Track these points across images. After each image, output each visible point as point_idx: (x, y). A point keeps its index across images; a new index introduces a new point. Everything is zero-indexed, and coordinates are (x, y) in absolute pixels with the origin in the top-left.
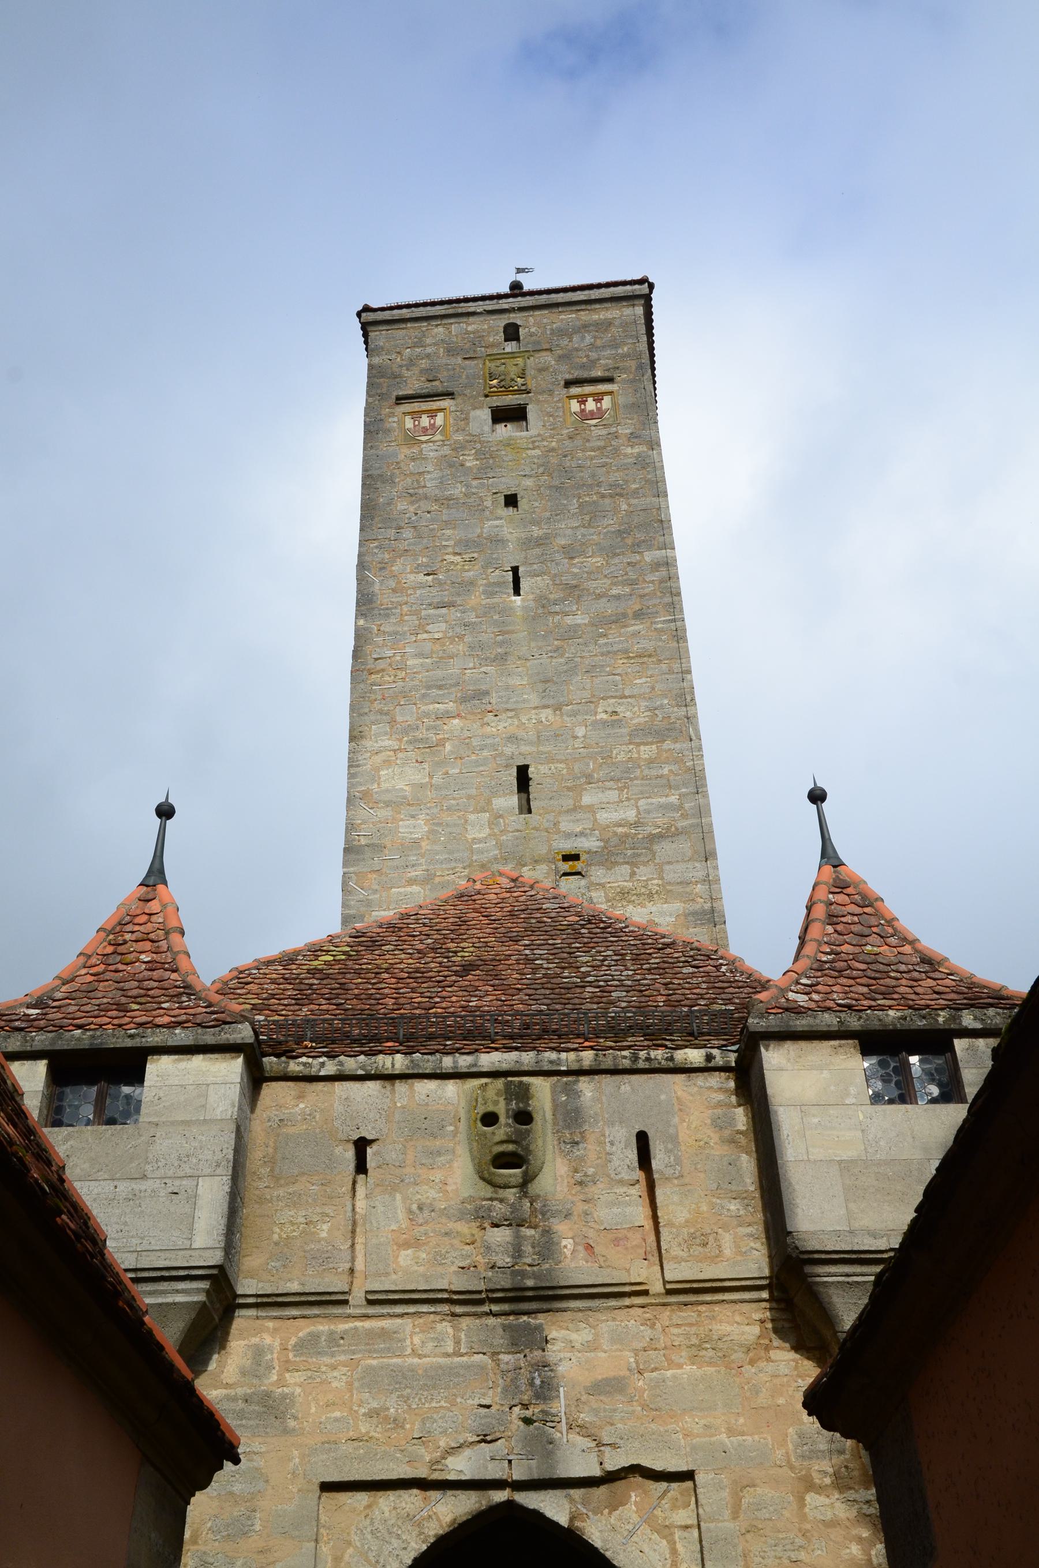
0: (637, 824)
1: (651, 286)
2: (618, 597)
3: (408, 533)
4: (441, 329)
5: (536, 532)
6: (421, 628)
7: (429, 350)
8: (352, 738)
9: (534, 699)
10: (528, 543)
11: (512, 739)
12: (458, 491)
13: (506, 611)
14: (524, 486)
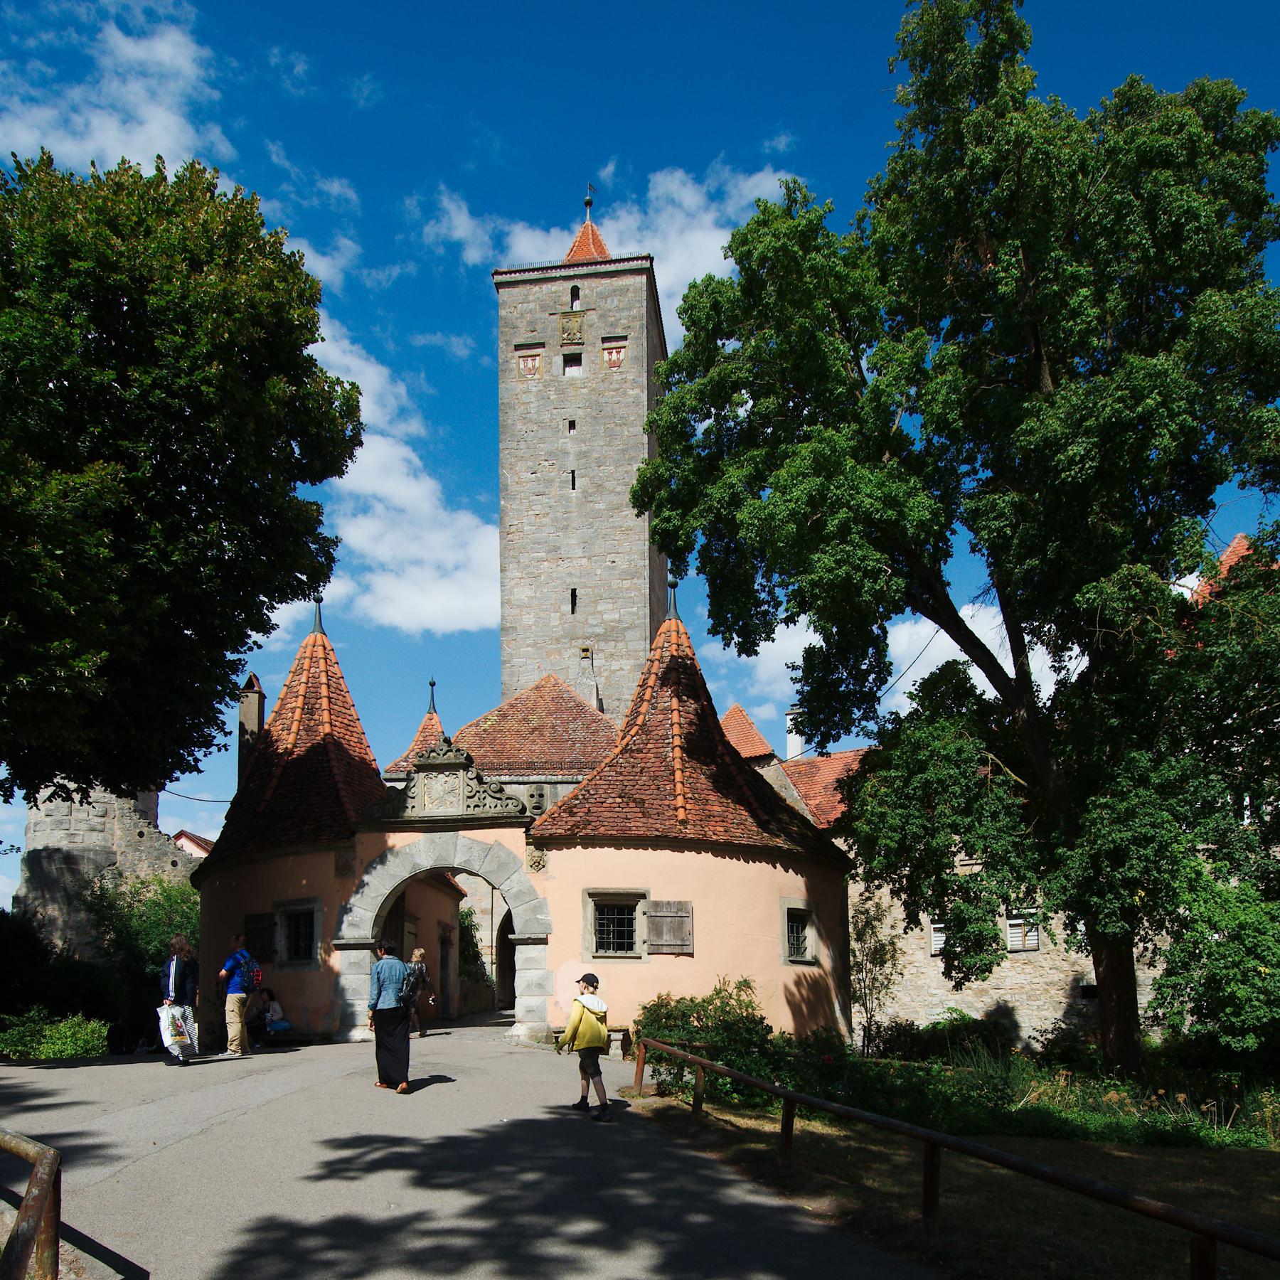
0: (619, 621)
1: (652, 259)
2: (619, 493)
3: (523, 445)
4: (536, 288)
5: (584, 448)
6: (529, 509)
7: (532, 306)
8: (502, 571)
9: (579, 552)
10: (582, 455)
11: (570, 574)
12: (546, 417)
13: (568, 499)
14: (578, 415)
